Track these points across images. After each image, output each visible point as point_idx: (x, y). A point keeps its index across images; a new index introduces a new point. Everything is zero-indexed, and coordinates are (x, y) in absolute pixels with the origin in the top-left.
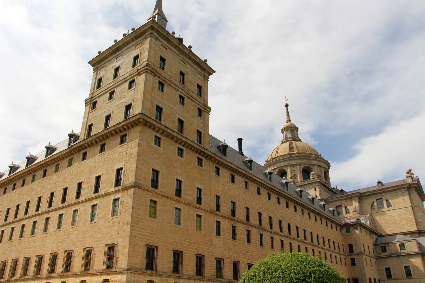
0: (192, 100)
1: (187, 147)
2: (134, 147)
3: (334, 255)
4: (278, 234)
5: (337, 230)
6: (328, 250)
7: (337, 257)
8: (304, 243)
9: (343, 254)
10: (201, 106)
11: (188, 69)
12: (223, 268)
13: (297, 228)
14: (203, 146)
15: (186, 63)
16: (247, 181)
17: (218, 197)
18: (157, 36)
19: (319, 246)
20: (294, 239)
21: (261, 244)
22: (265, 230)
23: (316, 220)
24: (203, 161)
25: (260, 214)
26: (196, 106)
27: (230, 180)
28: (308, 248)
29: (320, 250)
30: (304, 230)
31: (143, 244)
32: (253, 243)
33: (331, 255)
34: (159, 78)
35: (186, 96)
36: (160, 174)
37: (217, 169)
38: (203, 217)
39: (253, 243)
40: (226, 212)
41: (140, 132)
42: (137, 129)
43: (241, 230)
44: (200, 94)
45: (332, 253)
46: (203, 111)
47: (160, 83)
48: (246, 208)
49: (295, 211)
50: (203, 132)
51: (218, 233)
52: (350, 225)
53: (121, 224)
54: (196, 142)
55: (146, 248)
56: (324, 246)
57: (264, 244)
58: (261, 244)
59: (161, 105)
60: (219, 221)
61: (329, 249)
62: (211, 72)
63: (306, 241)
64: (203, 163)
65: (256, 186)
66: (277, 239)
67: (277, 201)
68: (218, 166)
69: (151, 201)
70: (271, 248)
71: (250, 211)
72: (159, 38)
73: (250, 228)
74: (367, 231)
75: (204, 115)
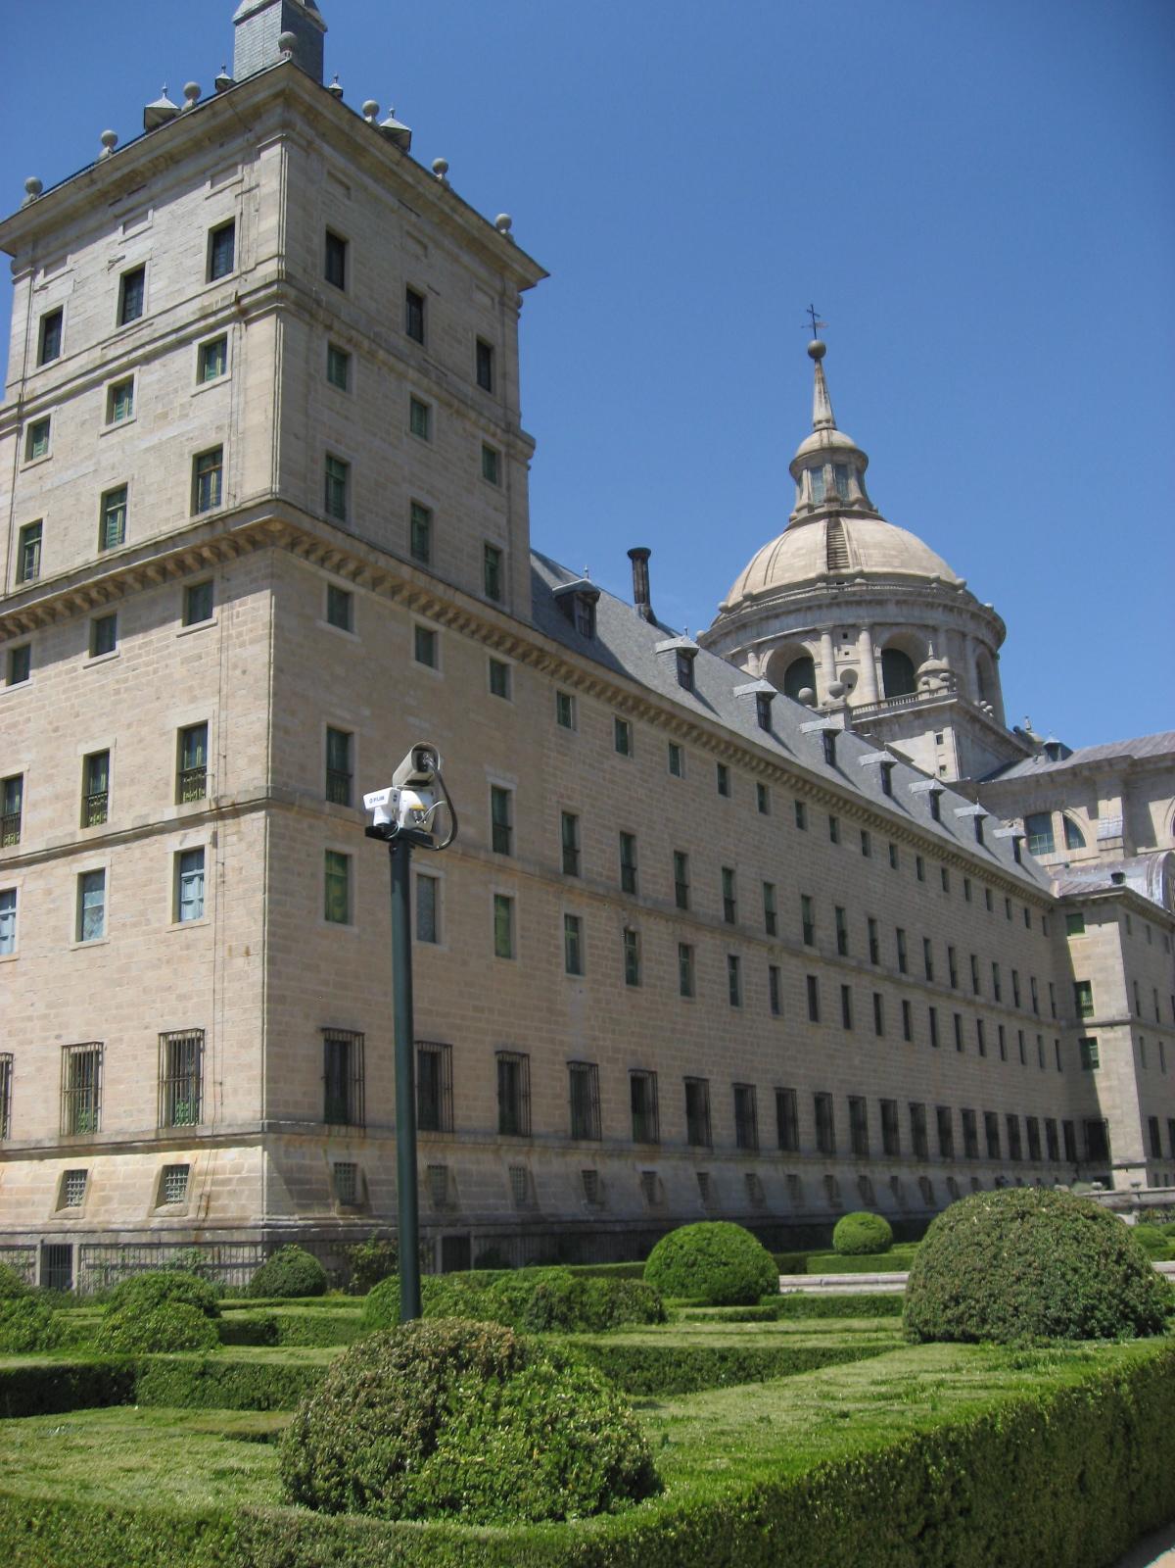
0: (458, 412)
1: (449, 623)
2: (253, 642)
3: (1012, 1027)
4: (796, 953)
5: (1028, 925)
6: (992, 1009)
7: (1026, 1036)
8: (898, 983)
9: (1050, 1019)
10: (494, 435)
11: (441, 276)
12: (597, 1101)
13: (872, 922)
14: (507, 609)
15: (431, 246)
16: (677, 740)
17: (570, 820)
18: (310, 133)
19: (957, 993)
20: (859, 970)
21: (735, 999)
22: (749, 940)
23: (945, 888)
24: (512, 670)
25: (728, 873)
26: (474, 437)
27: (611, 741)
28: (913, 1004)
29: (960, 1009)
30: (900, 932)
31: (310, 1027)
32: (703, 995)
33: (1001, 1028)
34: (329, 328)
35: (437, 398)
36: (356, 745)
37: (564, 701)
38: (517, 907)
39: (703, 995)
40: (601, 875)
41: (272, 576)
42: (257, 561)
43: (658, 942)
44: (485, 381)
45: (1005, 1022)
46: (503, 458)
47: (332, 348)
48: (676, 853)
49: (865, 852)
50: (506, 550)
51: (574, 967)
52: (1084, 903)
53: (222, 952)
54: (482, 595)
55: (321, 1039)
56: (976, 991)
57: (743, 996)
58: (735, 999)
59: (342, 452)
60: (577, 914)
61: (993, 1003)
62: (531, 275)
63: (904, 977)
64: (512, 682)
65: (714, 759)
66: (794, 975)
67: (793, 816)
68: (567, 689)
69: (330, 854)
70: (769, 1011)
71: (693, 866)
72: (318, 142)
73: (690, 936)
74: (1153, 926)
75: (508, 474)
